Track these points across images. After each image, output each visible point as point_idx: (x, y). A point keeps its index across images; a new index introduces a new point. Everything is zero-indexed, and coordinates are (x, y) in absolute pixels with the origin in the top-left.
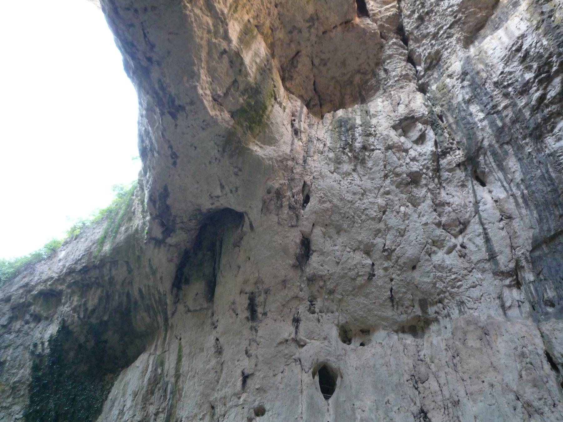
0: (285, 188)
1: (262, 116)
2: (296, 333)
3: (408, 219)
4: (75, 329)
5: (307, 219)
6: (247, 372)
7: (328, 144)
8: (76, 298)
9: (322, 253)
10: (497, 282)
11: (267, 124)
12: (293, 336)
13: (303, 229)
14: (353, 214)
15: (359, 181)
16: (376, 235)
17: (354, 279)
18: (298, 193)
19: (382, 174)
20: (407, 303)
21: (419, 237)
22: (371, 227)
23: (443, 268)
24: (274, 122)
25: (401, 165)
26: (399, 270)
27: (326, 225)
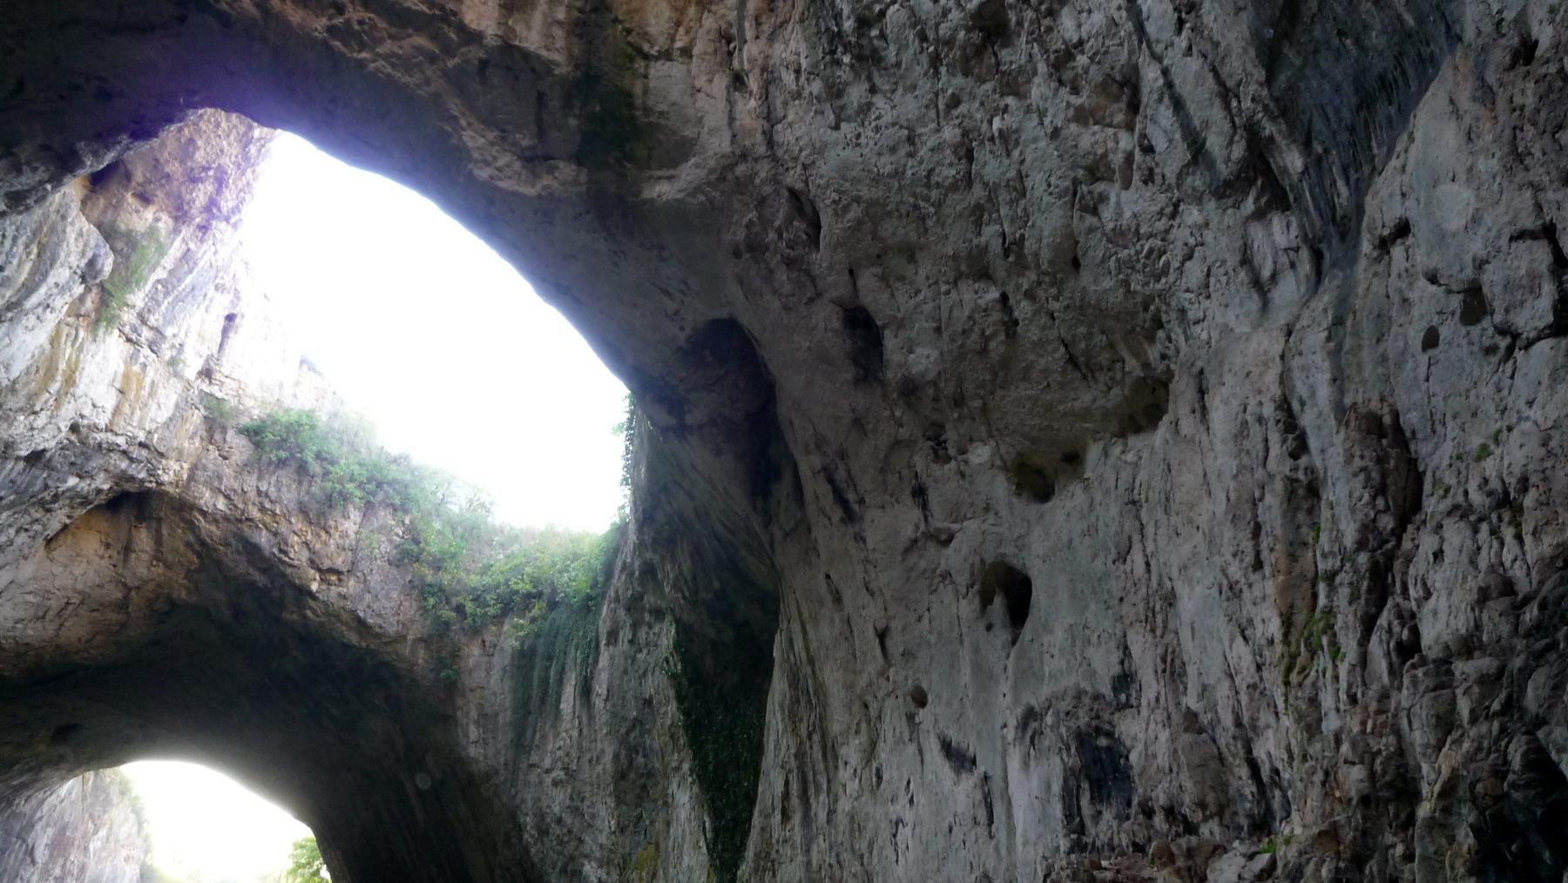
0: (756, 229)
1: (633, 118)
2: (926, 520)
3: (1017, 143)
4: (688, 618)
5: (830, 267)
6: (881, 626)
7: (804, 64)
8: (668, 567)
9: (901, 324)
10: (1231, 217)
11: (650, 124)
12: (922, 527)
13: (834, 294)
14: (912, 200)
15: (898, 107)
16: (978, 224)
17: (983, 351)
18: (789, 221)
19: (924, 59)
20: (1104, 358)
21: (1053, 180)
22: (958, 208)
23: (1122, 234)
24: (663, 107)
25: (945, 13)
26: (1053, 284)
27: (879, 256)
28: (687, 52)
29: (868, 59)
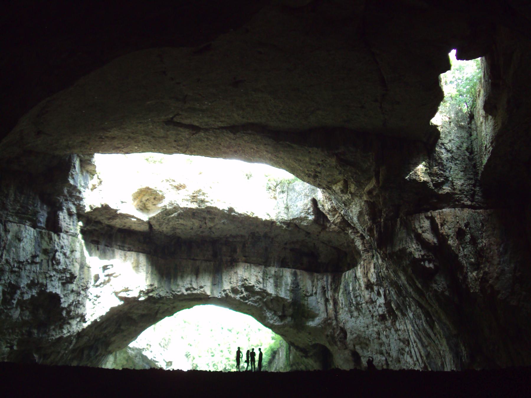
16: (381, 346)
18: (340, 333)
24: (311, 307)
25: (375, 312)
28: (316, 293)
29: (358, 309)
